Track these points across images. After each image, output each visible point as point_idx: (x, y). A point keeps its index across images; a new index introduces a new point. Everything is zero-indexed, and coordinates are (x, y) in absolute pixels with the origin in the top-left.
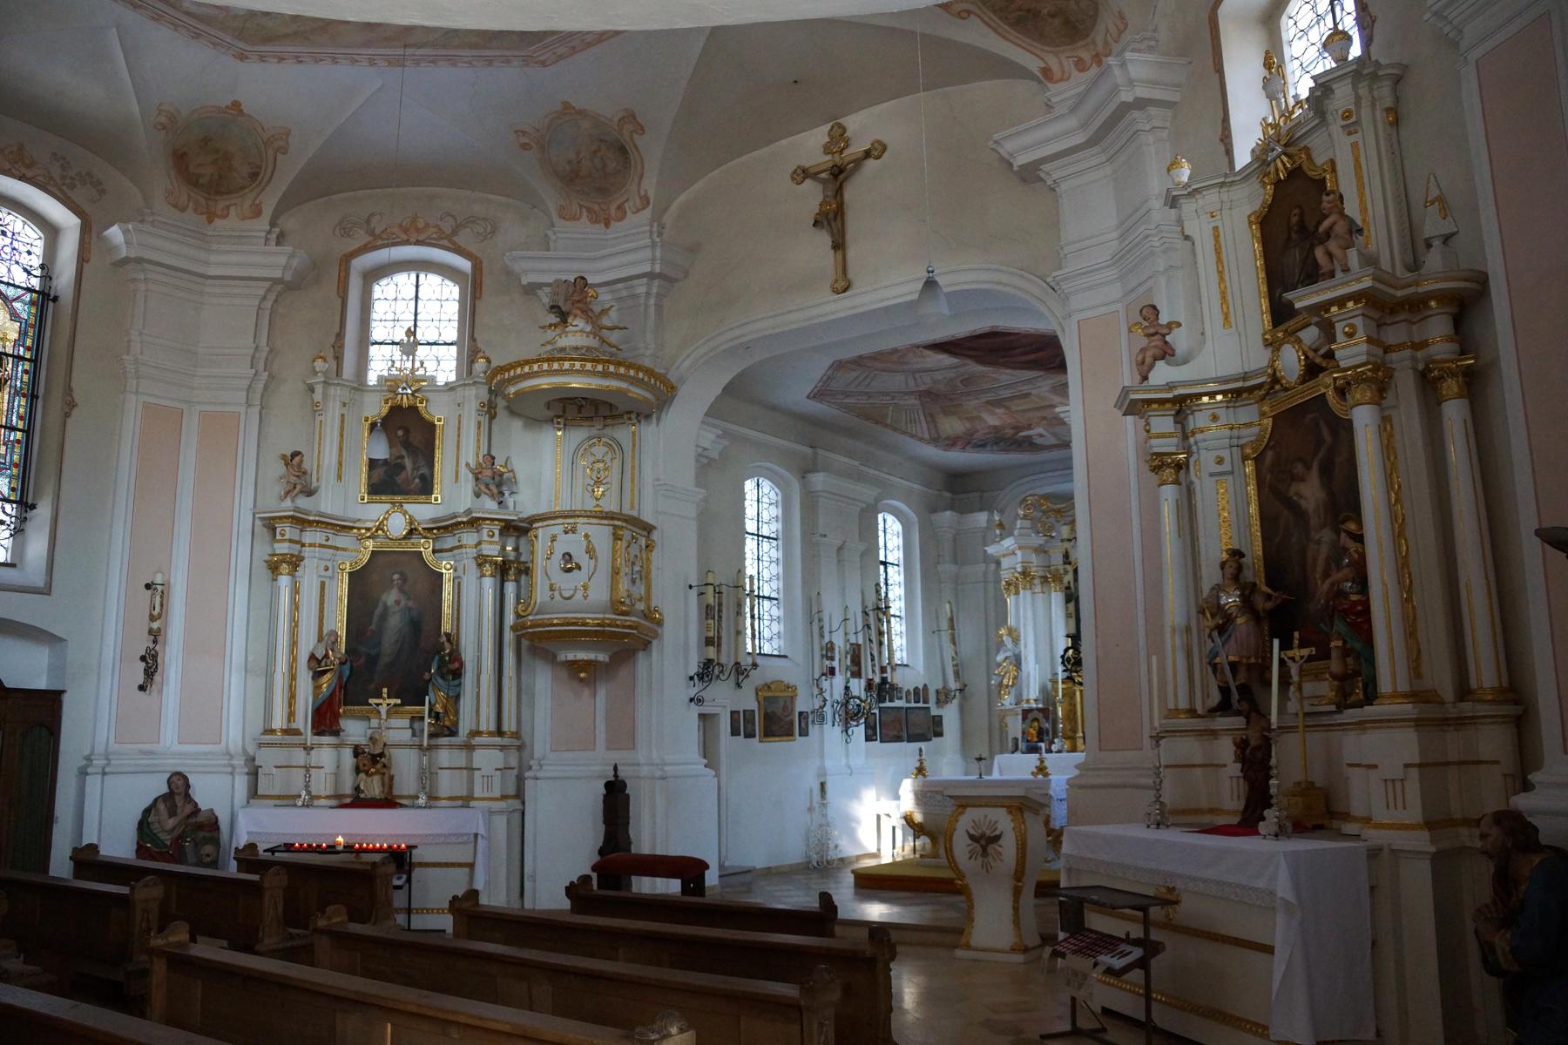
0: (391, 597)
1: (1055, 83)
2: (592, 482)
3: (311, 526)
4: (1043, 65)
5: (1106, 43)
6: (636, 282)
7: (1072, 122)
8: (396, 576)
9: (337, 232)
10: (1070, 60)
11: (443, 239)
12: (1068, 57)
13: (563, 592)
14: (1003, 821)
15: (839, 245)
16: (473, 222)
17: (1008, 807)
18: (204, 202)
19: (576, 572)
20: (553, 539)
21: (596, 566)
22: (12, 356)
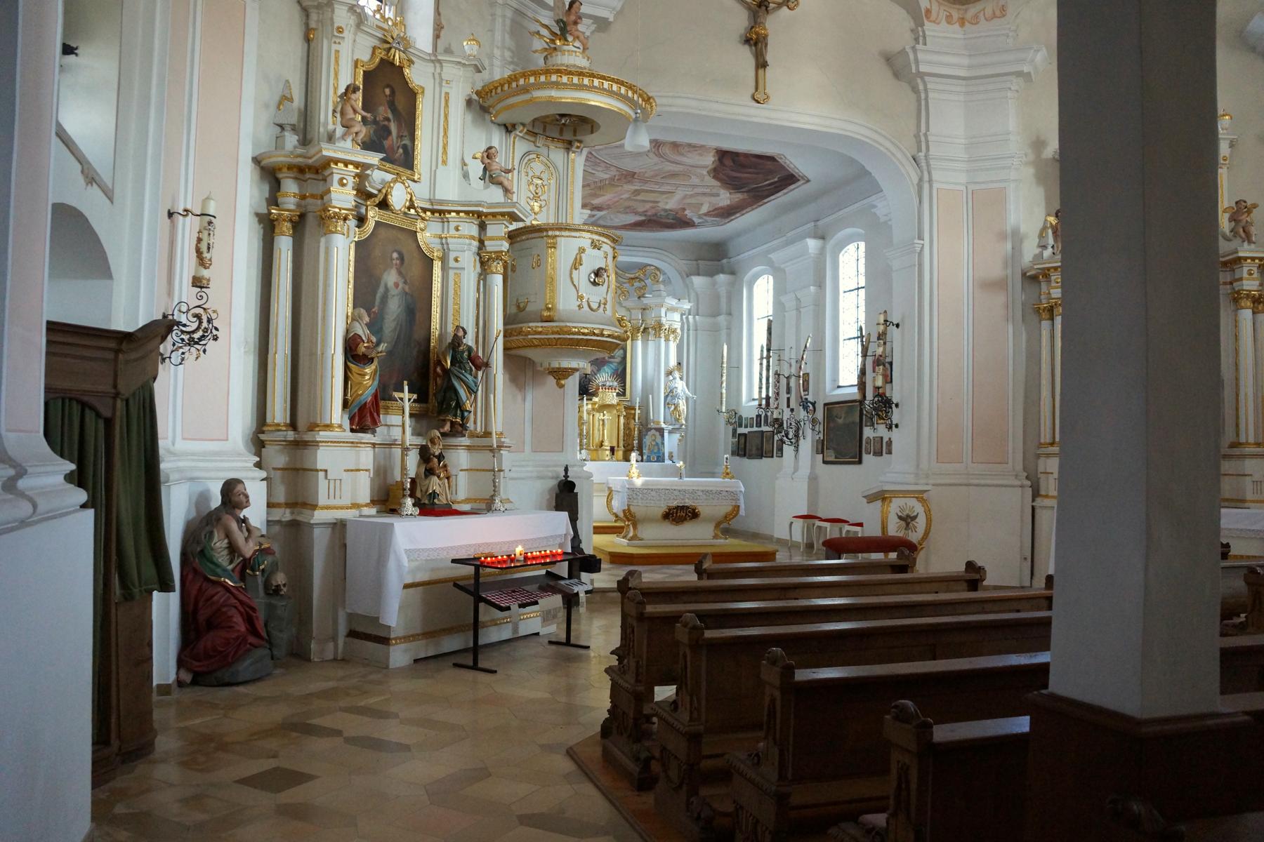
0: (391, 278)
1: (931, 21)
4: (929, 7)
5: (976, 16)
7: (966, 61)
10: (945, 13)
12: (944, 10)
13: (592, 304)
14: (918, 508)
15: (761, 64)
17: (916, 497)
20: (582, 250)
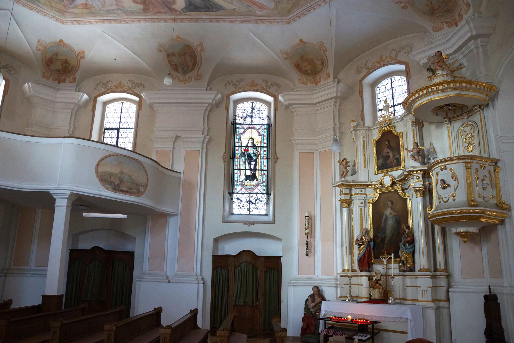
0: (388, 212)
2: (467, 145)
3: (354, 187)
6: (469, 44)
8: (389, 203)
9: (356, 73)
11: (393, 60)
16: (403, 49)
18: (312, 79)
19: (448, 188)
21: (458, 184)
22: (260, 147)
